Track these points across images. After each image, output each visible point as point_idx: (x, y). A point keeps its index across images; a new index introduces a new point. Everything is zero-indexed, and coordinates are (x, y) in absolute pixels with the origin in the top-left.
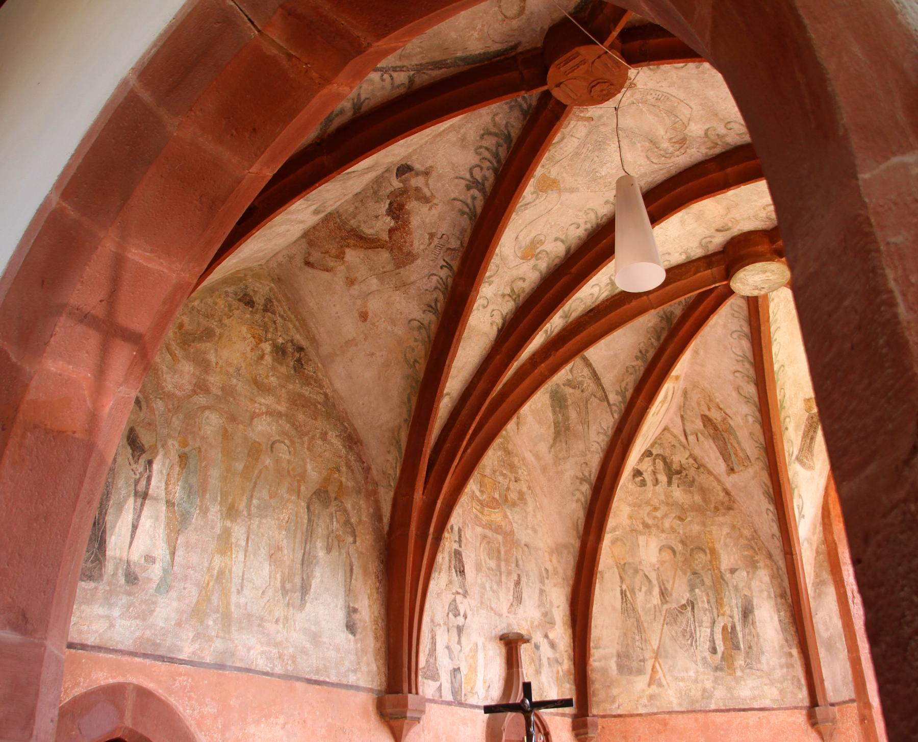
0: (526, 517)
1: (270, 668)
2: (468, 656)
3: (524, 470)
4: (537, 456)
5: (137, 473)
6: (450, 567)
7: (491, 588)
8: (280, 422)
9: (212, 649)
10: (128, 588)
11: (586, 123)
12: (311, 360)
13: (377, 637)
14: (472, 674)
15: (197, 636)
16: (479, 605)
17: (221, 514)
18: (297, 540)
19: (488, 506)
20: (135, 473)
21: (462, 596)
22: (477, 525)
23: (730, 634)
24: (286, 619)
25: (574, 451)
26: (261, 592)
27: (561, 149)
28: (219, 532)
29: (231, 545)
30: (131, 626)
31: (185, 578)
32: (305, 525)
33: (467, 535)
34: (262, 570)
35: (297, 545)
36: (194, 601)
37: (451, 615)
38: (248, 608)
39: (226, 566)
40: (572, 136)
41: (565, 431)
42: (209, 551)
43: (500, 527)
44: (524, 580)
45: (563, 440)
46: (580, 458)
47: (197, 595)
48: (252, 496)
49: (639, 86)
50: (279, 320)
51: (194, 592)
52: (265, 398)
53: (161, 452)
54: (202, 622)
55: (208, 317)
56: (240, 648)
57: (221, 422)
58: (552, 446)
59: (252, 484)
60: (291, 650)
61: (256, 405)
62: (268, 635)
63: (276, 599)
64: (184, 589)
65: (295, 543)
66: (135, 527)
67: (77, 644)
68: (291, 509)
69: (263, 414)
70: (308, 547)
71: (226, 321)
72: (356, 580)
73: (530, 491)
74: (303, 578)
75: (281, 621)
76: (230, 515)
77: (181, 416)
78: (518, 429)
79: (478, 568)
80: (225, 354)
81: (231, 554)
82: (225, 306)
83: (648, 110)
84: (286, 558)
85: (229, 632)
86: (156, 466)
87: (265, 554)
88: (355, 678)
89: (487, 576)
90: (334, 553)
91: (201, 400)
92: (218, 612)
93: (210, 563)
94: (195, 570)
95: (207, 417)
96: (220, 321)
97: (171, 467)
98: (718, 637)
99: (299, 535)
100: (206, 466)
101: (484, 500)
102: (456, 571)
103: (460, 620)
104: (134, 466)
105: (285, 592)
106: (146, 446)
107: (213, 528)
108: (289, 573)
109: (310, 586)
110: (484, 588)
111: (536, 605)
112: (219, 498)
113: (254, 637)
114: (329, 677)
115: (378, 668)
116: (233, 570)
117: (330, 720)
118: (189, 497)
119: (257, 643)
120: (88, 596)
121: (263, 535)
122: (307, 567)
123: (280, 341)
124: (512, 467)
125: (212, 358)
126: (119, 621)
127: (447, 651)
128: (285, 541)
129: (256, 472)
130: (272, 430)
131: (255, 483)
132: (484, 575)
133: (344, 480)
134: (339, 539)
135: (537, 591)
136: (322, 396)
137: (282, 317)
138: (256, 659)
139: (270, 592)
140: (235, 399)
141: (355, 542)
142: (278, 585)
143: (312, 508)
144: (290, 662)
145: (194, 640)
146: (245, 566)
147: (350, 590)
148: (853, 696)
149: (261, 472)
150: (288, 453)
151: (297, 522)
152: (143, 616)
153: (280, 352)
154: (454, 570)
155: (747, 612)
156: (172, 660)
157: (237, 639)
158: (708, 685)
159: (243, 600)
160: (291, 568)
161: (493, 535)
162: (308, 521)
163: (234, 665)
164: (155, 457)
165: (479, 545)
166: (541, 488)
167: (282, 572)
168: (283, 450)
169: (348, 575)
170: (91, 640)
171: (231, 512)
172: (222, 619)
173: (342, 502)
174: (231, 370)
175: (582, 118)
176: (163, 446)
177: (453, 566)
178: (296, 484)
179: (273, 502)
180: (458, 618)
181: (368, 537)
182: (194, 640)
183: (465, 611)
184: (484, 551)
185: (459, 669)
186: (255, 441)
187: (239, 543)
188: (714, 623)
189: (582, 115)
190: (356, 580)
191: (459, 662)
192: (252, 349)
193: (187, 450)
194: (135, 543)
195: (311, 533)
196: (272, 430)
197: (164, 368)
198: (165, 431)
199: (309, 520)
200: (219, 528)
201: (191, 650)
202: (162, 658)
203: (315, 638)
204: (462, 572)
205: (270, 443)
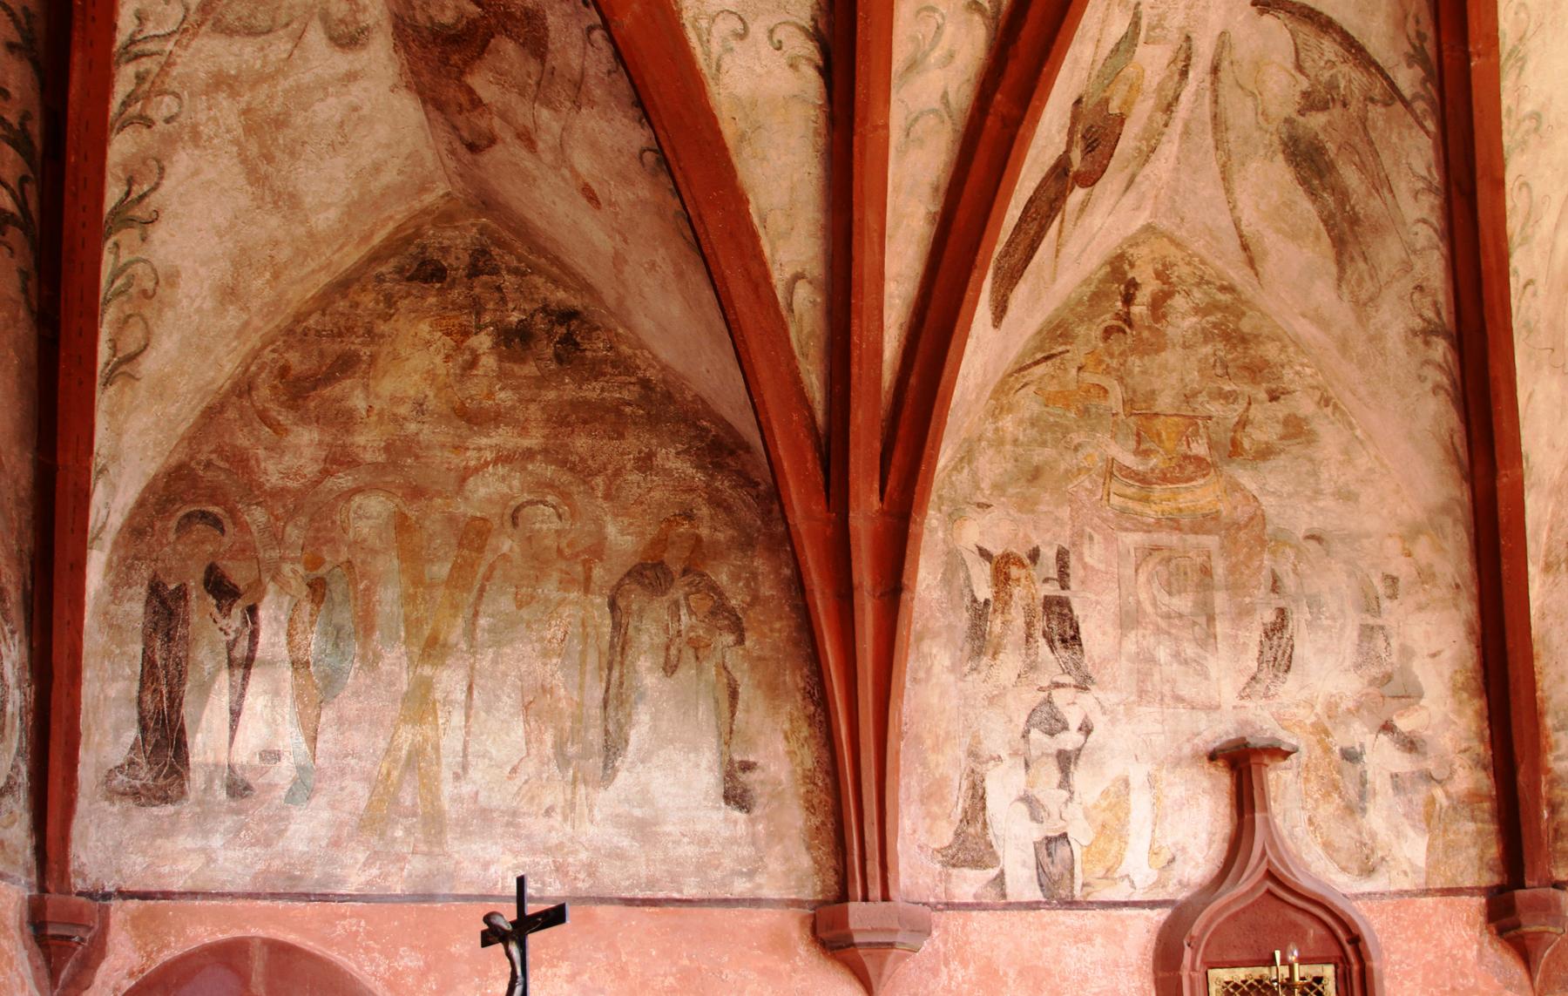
0: (1315, 474)
1: (537, 889)
2: (1095, 807)
3: (1302, 365)
4: (1322, 322)
5: (229, 631)
6: (1029, 636)
7: (1177, 655)
8: (530, 467)
9: (405, 873)
10: (233, 804)
12: (598, 328)
13: (813, 806)
14: (1111, 841)
15: (374, 856)
16: (1133, 698)
17: (410, 659)
18: (589, 668)
19: (1164, 479)
20: (226, 634)
21: (1074, 690)
22: (1126, 530)
24: (572, 805)
25: (1385, 270)
26: (509, 769)
28: (405, 688)
29: (434, 704)
30: (245, 858)
31: (342, 772)
32: (608, 638)
33: (1087, 559)
34: (508, 735)
35: (588, 677)
36: (363, 805)
37: (1035, 734)
38: (481, 798)
39: (426, 740)
41: (1352, 230)
42: (387, 722)
43: (1215, 516)
44: (1299, 618)
45: (1355, 255)
46: (1403, 281)
47: (367, 795)
48: (476, 614)
50: (509, 281)
51: (362, 791)
52: (488, 436)
53: (271, 588)
54: (382, 835)
55: (340, 335)
56: (466, 864)
57: (391, 506)
58: (1340, 279)
59: (475, 592)
60: (584, 856)
61: (469, 454)
62: (528, 837)
63: (545, 776)
64: (342, 789)
65: (583, 673)
66: (235, 714)
67: (156, 893)
68: (568, 616)
69: (487, 464)
70: (616, 674)
71: (383, 327)
72: (748, 711)
73: (1329, 410)
74: (607, 732)
75: (558, 810)
76: (429, 656)
77: (303, 520)
78: (1257, 275)
79: (1128, 620)
80: (387, 386)
81: (436, 718)
82: (377, 303)
84: (563, 704)
85: (440, 844)
86: (262, 613)
87: (512, 706)
88: (748, 885)
89: (1158, 631)
90: (686, 672)
91: (344, 481)
92: (415, 815)
93: (392, 741)
94: (360, 758)
95: (359, 507)
96: (370, 331)
97: (296, 607)
99: (592, 659)
100: (367, 589)
101: (1152, 470)
102: (1051, 643)
103: (1070, 740)
104: (223, 623)
105: (563, 759)
106: (242, 586)
107: (391, 684)
108: (572, 728)
109: (627, 742)
110: (1153, 660)
111: (1348, 663)
112: (403, 634)
113: (496, 843)
114: (680, 891)
115: (816, 861)
116: (442, 743)
117: (686, 962)
118: (336, 645)
119: (503, 853)
120: (166, 826)
121: (505, 675)
122: (617, 708)
123: (515, 317)
124: (1256, 371)
125: (359, 402)
126: (223, 852)
127: (1023, 807)
128: (559, 674)
129: (482, 570)
130: (511, 488)
131: (482, 590)
132: (1148, 632)
133: (704, 532)
134: (697, 646)
135: (1352, 633)
136: (636, 388)
137: (515, 272)
138: (504, 878)
139: (530, 768)
140: (417, 457)
141: (740, 641)
142: (548, 750)
143: (622, 603)
144: (582, 876)
145: (367, 864)
146: (468, 733)
147: (731, 732)
149: (492, 568)
150: (555, 519)
151: (586, 636)
153: (514, 340)
154: (1042, 642)
156: (324, 898)
157: (458, 852)
159: (466, 789)
160: (578, 718)
161: (1185, 540)
162: (614, 628)
163: (454, 892)
164: (260, 599)
165: (1130, 571)
166: (1354, 393)
167: (555, 728)
168: (544, 520)
169: (725, 705)
170: (177, 885)
171: (433, 649)
172: (425, 825)
173: (702, 575)
174: (403, 410)
176: (273, 578)
177: (1038, 634)
178: (579, 568)
179: (525, 613)
180: (1062, 736)
181: (777, 625)
182: (367, 864)
183: (1086, 717)
184: (1149, 582)
185: (1064, 836)
186: (474, 518)
187: (452, 697)
190: (748, 711)
191: (1062, 823)
192: (447, 358)
193: (322, 572)
194: (239, 736)
195: (623, 648)
196: (511, 488)
197: (261, 453)
198: (276, 554)
199: (617, 626)
200: (405, 681)
201: (363, 879)
202: (306, 897)
203: (644, 830)
204: (1071, 639)
205: (509, 511)
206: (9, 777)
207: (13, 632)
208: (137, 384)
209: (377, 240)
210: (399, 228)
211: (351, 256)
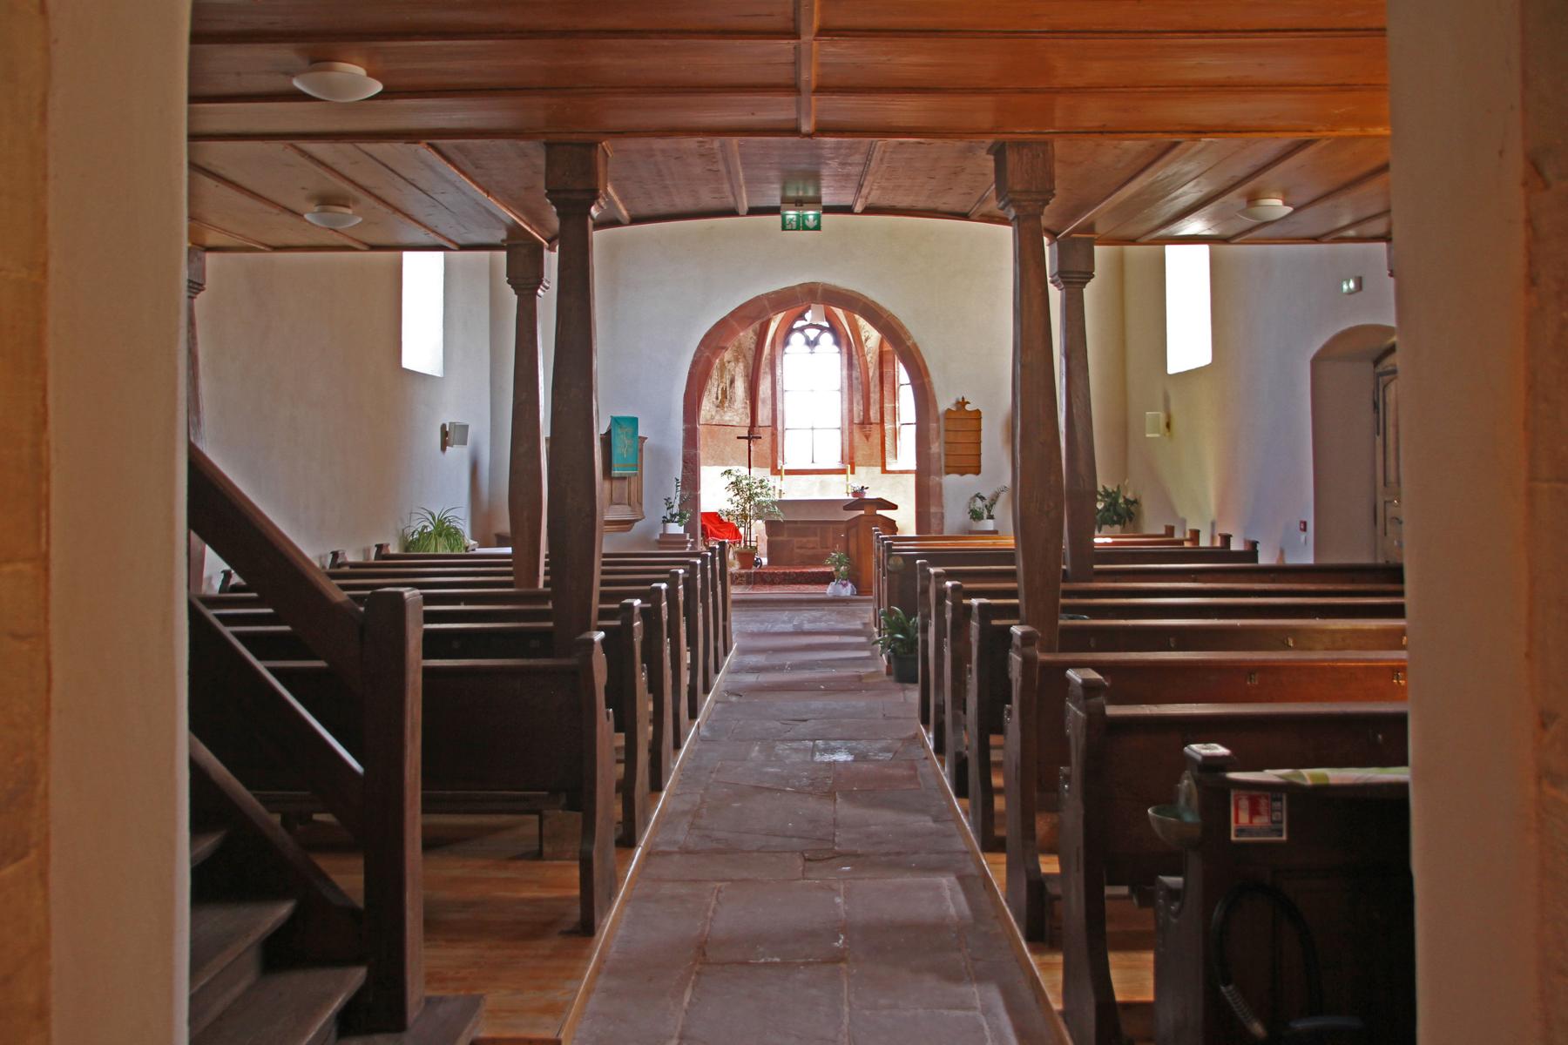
23: (724, 392)
98: (720, 392)
148: (770, 424)
155: (732, 382)
158: (714, 413)
188: (718, 385)
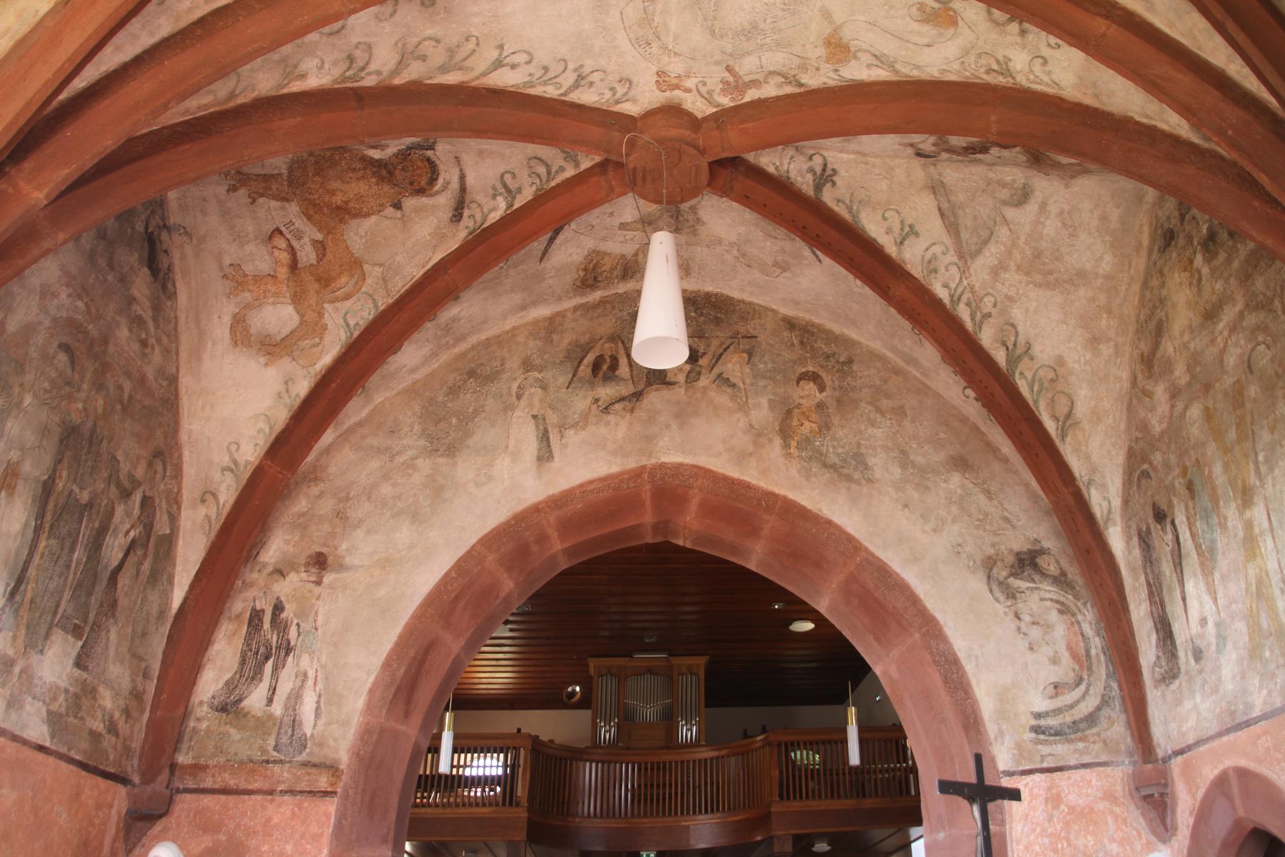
11: (737, 69)
27: (784, 66)
40: (762, 67)
49: (655, 69)
66: (1184, 599)
83: (668, 35)
86: (1177, 522)
152: (1215, 690)
156: (1247, 724)
175: (734, 76)
189: (731, 79)
194: (1190, 616)
206: (1103, 696)
207: (1085, 604)
208: (1081, 424)
209: (1145, 242)
210: (1151, 225)
211: (1140, 263)
